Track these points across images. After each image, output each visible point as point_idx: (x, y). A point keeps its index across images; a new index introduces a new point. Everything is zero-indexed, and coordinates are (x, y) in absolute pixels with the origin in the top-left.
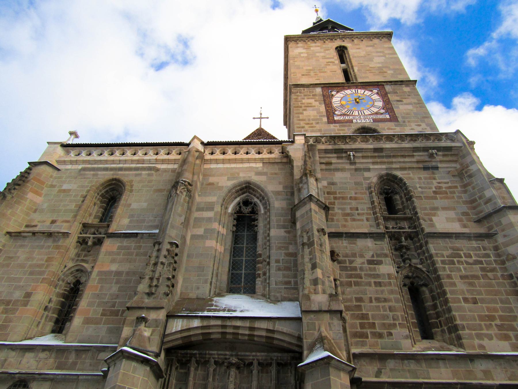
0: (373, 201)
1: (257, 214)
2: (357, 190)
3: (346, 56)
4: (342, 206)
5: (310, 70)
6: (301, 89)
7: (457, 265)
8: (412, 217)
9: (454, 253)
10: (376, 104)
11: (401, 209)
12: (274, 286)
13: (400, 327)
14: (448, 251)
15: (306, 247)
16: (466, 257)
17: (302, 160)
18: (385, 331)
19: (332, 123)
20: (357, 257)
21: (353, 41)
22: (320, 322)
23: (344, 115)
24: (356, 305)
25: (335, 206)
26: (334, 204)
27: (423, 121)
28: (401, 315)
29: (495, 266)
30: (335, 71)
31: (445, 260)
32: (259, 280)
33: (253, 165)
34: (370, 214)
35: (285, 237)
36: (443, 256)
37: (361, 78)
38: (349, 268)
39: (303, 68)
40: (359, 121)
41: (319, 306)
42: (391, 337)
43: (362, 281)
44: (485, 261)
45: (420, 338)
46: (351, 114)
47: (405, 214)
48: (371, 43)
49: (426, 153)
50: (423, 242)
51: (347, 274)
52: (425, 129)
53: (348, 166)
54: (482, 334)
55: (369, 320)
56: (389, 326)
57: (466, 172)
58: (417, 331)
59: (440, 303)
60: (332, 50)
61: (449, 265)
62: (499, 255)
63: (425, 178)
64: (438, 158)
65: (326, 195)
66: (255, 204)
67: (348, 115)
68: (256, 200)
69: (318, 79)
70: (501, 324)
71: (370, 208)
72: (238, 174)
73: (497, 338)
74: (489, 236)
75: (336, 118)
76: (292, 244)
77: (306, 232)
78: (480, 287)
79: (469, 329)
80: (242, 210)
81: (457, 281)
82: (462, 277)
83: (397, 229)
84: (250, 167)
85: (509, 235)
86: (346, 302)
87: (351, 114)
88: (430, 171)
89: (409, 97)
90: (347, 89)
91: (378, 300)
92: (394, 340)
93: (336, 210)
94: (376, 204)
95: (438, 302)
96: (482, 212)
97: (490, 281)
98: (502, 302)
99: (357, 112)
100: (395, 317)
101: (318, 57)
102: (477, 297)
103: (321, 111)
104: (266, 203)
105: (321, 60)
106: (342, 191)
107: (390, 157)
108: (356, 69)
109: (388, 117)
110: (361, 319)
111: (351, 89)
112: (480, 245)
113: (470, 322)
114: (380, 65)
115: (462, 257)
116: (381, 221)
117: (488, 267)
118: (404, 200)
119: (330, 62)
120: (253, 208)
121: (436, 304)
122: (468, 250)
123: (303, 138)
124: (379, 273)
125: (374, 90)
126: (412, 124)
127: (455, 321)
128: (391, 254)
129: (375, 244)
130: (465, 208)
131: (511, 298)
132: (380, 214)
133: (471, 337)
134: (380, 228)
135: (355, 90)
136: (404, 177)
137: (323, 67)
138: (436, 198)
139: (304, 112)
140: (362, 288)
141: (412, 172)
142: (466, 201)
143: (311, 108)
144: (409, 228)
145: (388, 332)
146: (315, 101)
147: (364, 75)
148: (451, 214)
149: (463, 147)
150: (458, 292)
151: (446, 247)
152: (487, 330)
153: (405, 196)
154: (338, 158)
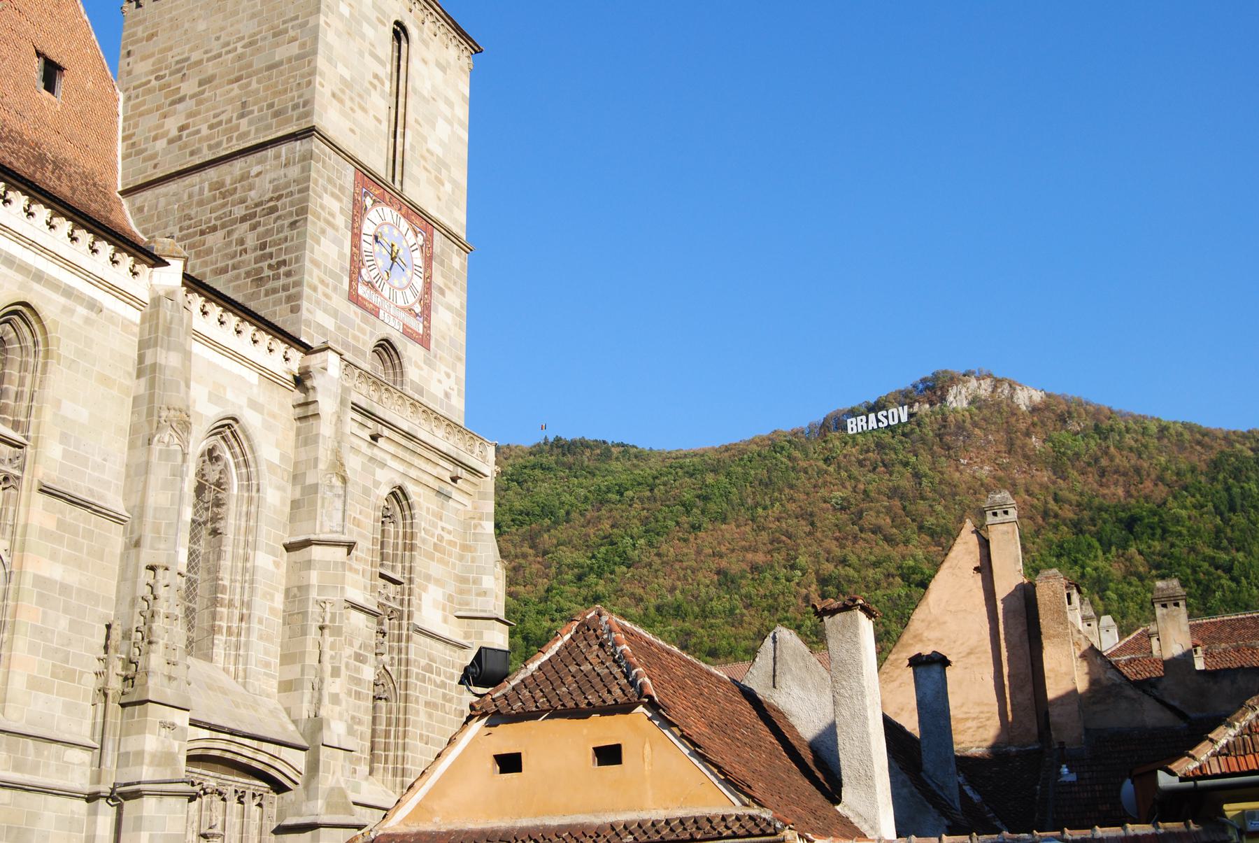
1: (224, 489)
15: (326, 631)
40: (386, 321)
47: (393, 568)
50: (405, 632)
52: (453, 390)
53: (364, 447)
66: (226, 466)
68: (227, 455)
75: (362, 290)
81: (421, 708)
82: (427, 704)
88: (441, 499)
95: (393, 729)
101: (363, 36)
104: (249, 479)
114: (439, 151)
121: (390, 730)
125: (419, 235)
129: (367, 627)
130: (452, 587)
138: (433, 559)
149: (489, 479)
153: (405, 537)
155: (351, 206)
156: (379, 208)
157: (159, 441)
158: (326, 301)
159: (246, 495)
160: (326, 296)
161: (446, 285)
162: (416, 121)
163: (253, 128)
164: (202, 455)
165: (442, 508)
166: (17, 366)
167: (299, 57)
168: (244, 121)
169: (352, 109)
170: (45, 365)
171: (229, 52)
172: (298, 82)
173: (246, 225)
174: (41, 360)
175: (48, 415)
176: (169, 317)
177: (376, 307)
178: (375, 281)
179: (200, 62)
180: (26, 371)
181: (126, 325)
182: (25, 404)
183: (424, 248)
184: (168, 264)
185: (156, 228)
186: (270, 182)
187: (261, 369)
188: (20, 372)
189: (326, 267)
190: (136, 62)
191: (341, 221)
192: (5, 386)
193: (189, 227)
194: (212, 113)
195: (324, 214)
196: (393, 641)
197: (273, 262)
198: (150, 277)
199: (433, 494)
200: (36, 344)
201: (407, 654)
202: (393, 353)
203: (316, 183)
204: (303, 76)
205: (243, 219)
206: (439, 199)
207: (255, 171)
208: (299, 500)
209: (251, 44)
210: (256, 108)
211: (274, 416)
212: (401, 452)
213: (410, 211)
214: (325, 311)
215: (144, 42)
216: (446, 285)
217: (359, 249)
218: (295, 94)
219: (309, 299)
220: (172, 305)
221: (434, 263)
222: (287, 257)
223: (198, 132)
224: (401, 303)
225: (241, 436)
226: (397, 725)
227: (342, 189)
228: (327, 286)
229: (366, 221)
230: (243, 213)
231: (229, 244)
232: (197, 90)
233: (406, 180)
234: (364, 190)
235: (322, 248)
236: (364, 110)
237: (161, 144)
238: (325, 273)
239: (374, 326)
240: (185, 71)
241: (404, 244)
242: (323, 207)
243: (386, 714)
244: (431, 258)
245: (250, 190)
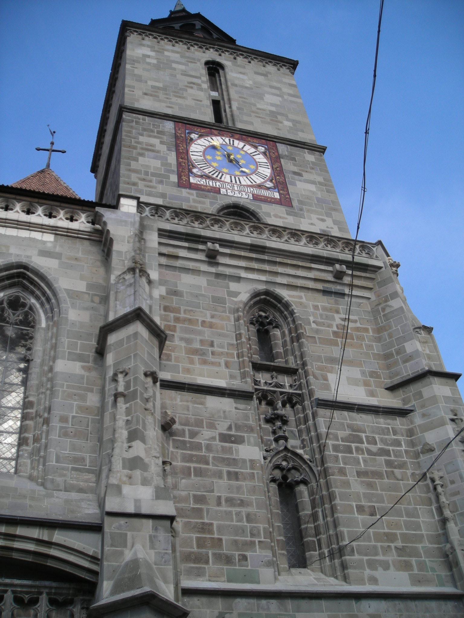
0: (240, 334)
1: (33, 327)
2: (216, 310)
3: (220, 80)
4: (187, 336)
5: (158, 88)
6: (141, 117)
7: (355, 455)
8: (297, 370)
9: (354, 435)
10: (260, 170)
11: (281, 352)
12: (54, 463)
13: (260, 548)
14: (345, 430)
15: (120, 400)
16: (368, 443)
17: (128, 242)
18: (237, 553)
20: (203, 428)
21: (235, 58)
22: (135, 533)
23: (208, 177)
24: (193, 508)
25: (176, 334)
26: (174, 329)
27: (329, 215)
28: (264, 528)
29: (405, 459)
30: (201, 101)
31: (339, 445)
32: (26, 450)
34: (232, 355)
35: (82, 377)
36: (336, 438)
37: (242, 122)
38: (188, 445)
39: (146, 82)
40: (230, 193)
41: (135, 506)
42: (244, 563)
43: (208, 469)
44: (393, 450)
45: (286, 566)
46: (218, 178)
47: (287, 362)
48: (262, 69)
49: (330, 268)
50: (309, 413)
51: (185, 454)
52: (332, 228)
53: (204, 267)
54: (377, 561)
55: (213, 534)
56: (242, 545)
57: (383, 309)
58: (283, 554)
59: (322, 511)
60: (198, 64)
61: (344, 453)
62: (412, 444)
63: (325, 309)
64: (347, 280)
65: (163, 312)
66: (31, 308)
67: (213, 179)
69: (170, 107)
70: (403, 546)
71: (232, 345)
72: (8, 247)
73: (394, 566)
74: (403, 413)
75: (192, 180)
76: (92, 391)
77: (124, 374)
78: (382, 490)
79: (359, 553)
80: (6, 315)
81: (352, 478)
82: (359, 474)
83: (272, 387)
84: (30, 239)
85: (430, 415)
86: (178, 502)
87: (218, 178)
89: (312, 171)
90: (216, 135)
91: (230, 501)
92: (249, 568)
93: (177, 342)
94: (244, 340)
96: (397, 374)
97: (397, 481)
98: (408, 515)
100: (255, 532)
101: (175, 69)
102: (376, 505)
103: (169, 161)
105: (179, 76)
106: (190, 308)
107: (275, 263)
108: (235, 105)
109: (277, 195)
110: (199, 532)
111: (223, 135)
112: (389, 426)
113: (362, 543)
114: (273, 109)
115: (363, 443)
116: (249, 369)
117: (396, 461)
118: (288, 339)
119: (194, 84)
120: (26, 314)
122: (373, 432)
123: (134, 203)
124: (236, 457)
125: (260, 147)
126: (312, 215)
127: (342, 541)
128: (258, 428)
129: (236, 408)
130: (375, 365)
131: (420, 508)
132: (248, 357)
133: (360, 565)
134: (246, 382)
135: (230, 140)
136: (292, 301)
137: (181, 89)
139: (140, 158)
140: (207, 481)
141: (305, 295)
142: (378, 354)
143: (151, 154)
144: (291, 386)
145: (242, 555)
146: (162, 143)
147: (245, 118)
148: (355, 372)
149: (383, 269)
150: (351, 496)
151: (343, 424)
152: (384, 555)
153: (290, 333)
154: (189, 249)
155: (174, 140)
158: (150, 189)
161: (300, 170)
165: (338, 304)
183: (268, 154)
187: (54, 230)
196: (300, 424)
199: (319, 296)
201: (316, 430)
212: (256, 265)
217: (188, 159)
221: (282, 160)
225: (36, 279)
226: (323, 504)
234: (187, 131)
235: (140, 162)
242: (138, 143)
243: (310, 497)
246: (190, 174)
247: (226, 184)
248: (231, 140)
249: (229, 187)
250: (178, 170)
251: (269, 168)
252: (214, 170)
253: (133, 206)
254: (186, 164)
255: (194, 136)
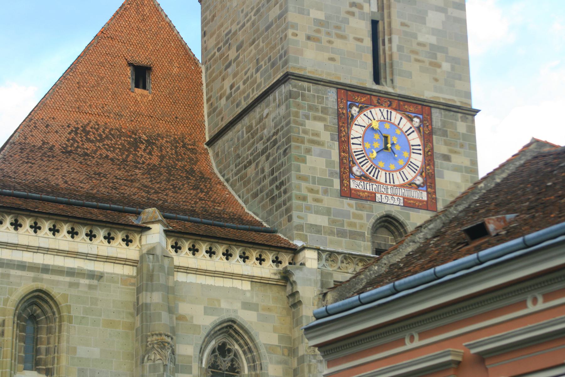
1: (238, 373)
6: (306, 85)
17: (313, 305)
19: (346, 197)
33: (237, 284)
40: (384, 201)
66: (235, 355)
67: (370, 180)
72: (219, 301)
75: (354, 184)
80: (219, 363)
99: (384, 172)
104: (254, 361)
109: (424, 196)
114: (433, 40)
135: (387, 111)
156: (367, 113)
157: (148, 359)
159: (253, 373)
160: (316, 200)
162: (403, 24)
163: (263, 79)
164: (213, 351)
166: (45, 331)
167: (280, 16)
168: (259, 74)
169: (330, 42)
170: (60, 327)
171: (248, 21)
172: (281, 37)
173: (263, 158)
174: (57, 324)
175: (64, 361)
176: (151, 267)
177: (371, 193)
178: (368, 173)
179: (235, 33)
180: (50, 333)
181: (125, 279)
182: (50, 356)
184: (149, 229)
185: (225, 168)
186: (273, 121)
187: (251, 279)
188: (47, 335)
189: (314, 178)
190: (208, 40)
191: (326, 136)
192: (38, 347)
193: (239, 164)
194: (244, 72)
195: (306, 137)
197: (277, 183)
198: (140, 240)
200: (54, 313)
202: (397, 224)
203: (297, 115)
204: (283, 32)
205: (263, 152)
206: (436, 80)
207: (266, 112)
208: (297, 368)
209: (258, 11)
210: (263, 63)
211: (269, 309)
213: (401, 103)
214: (317, 212)
215: (211, 23)
216: (451, 151)
218: (280, 47)
219: (299, 209)
220: (153, 258)
222: (283, 179)
223: (238, 88)
224: (399, 181)
225: (241, 331)
227: (325, 110)
228: (317, 192)
229: (354, 127)
230: (262, 147)
231: (257, 174)
232: (237, 54)
233: (397, 79)
235: (308, 164)
236: (343, 37)
237: (223, 101)
238: (314, 183)
239: (371, 208)
240: (230, 41)
241: (398, 132)
242: (305, 132)
244: (431, 134)
245: (264, 129)
246: (351, 176)
247: (382, 185)
248: (389, 111)
249: (383, 190)
250: (340, 171)
251: (420, 154)
252: (372, 165)
253: (314, 259)
254: (347, 159)
255: (355, 110)
